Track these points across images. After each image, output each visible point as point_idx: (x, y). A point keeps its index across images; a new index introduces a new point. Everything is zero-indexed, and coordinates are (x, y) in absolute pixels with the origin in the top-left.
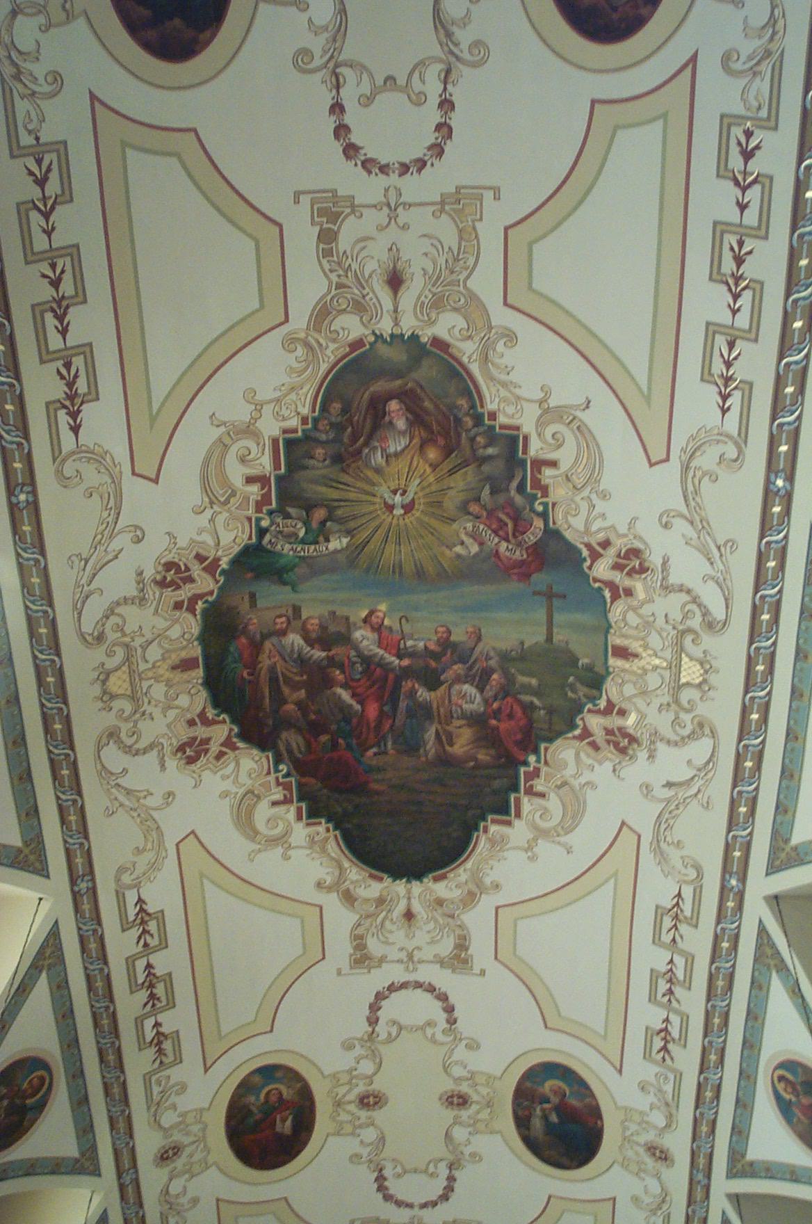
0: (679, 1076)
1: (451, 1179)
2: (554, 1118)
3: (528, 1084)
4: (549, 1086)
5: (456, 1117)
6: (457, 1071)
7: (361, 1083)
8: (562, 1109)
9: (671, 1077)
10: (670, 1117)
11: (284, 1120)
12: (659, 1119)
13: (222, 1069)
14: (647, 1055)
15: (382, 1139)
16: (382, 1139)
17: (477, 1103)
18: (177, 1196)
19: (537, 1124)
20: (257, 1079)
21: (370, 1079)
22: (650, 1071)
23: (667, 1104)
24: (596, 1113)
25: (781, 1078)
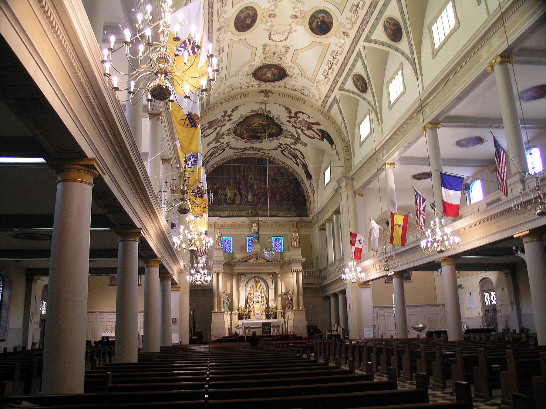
0: (358, 17)
1: (288, 35)
2: (320, 23)
3: (315, 14)
4: (320, 15)
5: (293, 21)
6: (297, 10)
7: (270, 11)
8: (323, 22)
9: (356, 17)
10: (352, 27)
11: (249, 20)
12: (349, 26)
13: (235, 8)
14: (351, 11)
15: (272, 26)
16: (272, 26)
17: (300, 18)
18: (220, 39)
19: (315, 24)
20: (244, 10)
21: (273, 10)
22: (350, 15)
23: (352, 23)
24: (332, 23)
25: (387, 21)
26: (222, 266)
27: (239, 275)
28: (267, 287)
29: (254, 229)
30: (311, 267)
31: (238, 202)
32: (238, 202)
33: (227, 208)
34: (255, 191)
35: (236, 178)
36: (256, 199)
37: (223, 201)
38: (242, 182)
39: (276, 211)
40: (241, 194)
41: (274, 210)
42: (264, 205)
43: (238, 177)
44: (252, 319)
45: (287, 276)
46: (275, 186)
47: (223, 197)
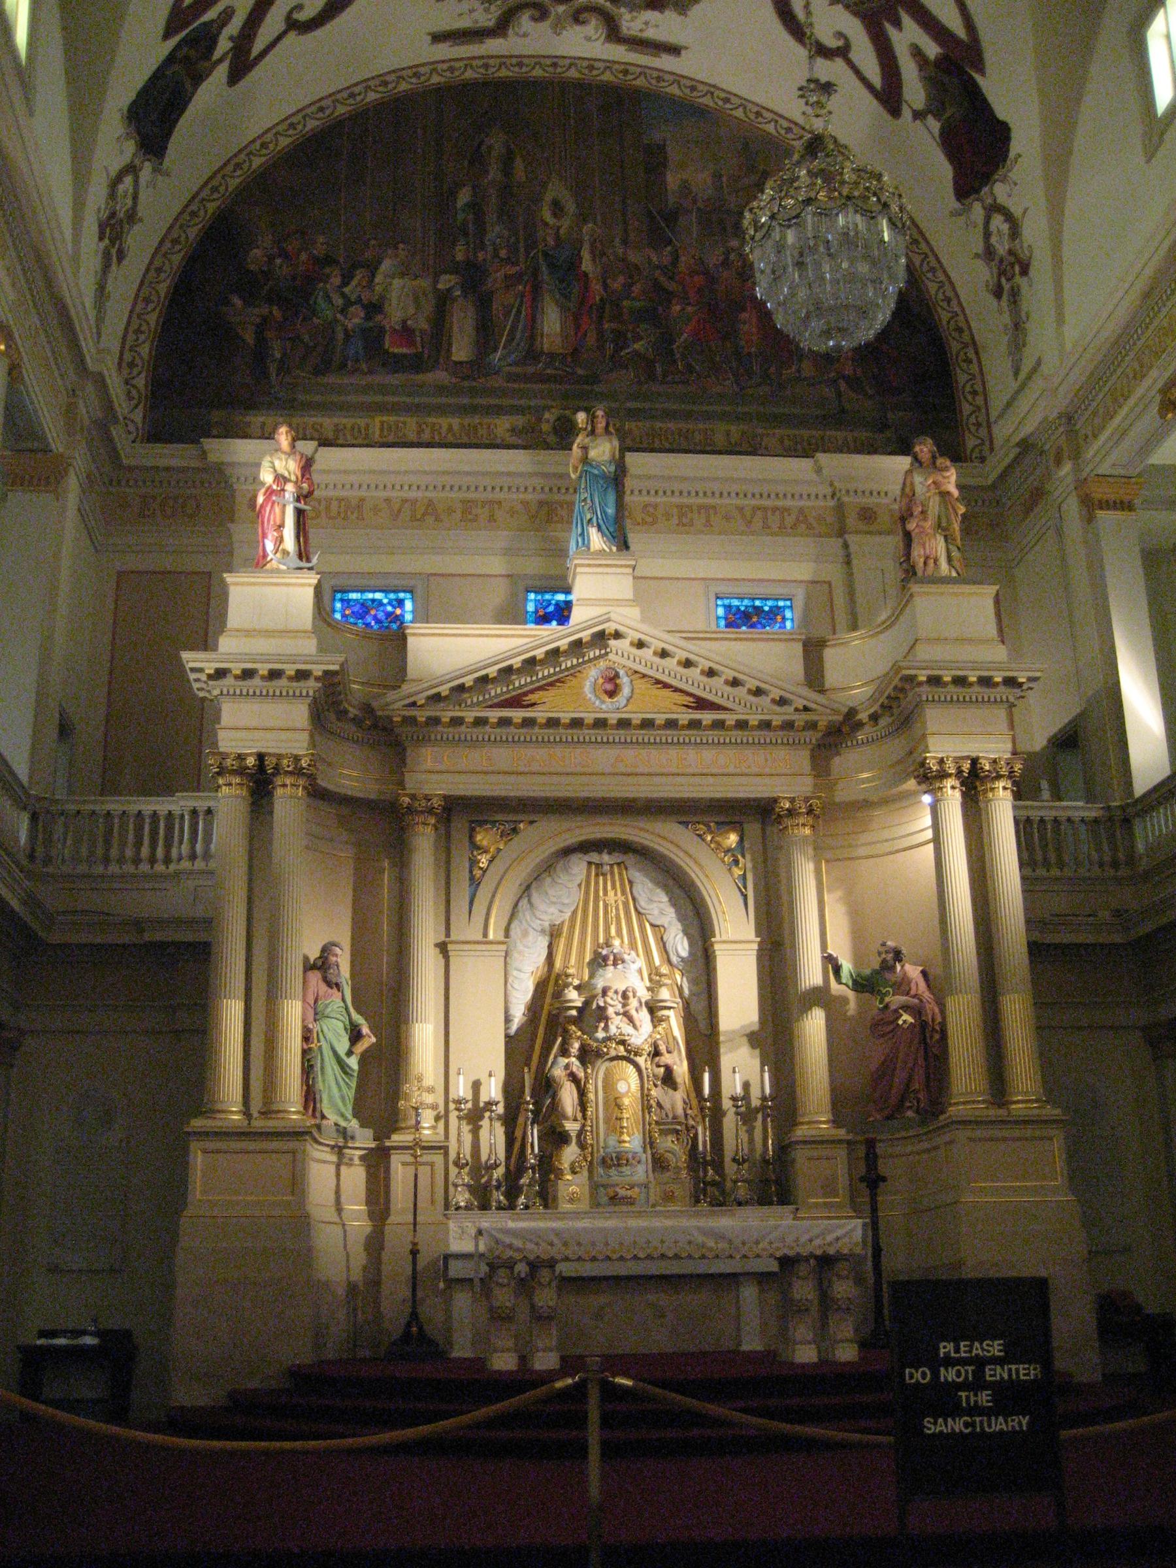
26: (300, 714)
27: (459, 826)
28: (695, 931)
29: (585, 460)
30: (1044, 784)
31: (461, 350)
32: (461, 350)
33: (383, 390)
34: (586, 287)
35: (453, 194)
36: (591, 340)
37: (357, 346)
38: (495, 232)
39: (739, 418)
40: (484, 303)
41: (724, 417)
42: (652, 377)
43: (464, 197)
44: (565, 1206)
45: (864, 838)
46: (726, 263)
47: (356, 319)
